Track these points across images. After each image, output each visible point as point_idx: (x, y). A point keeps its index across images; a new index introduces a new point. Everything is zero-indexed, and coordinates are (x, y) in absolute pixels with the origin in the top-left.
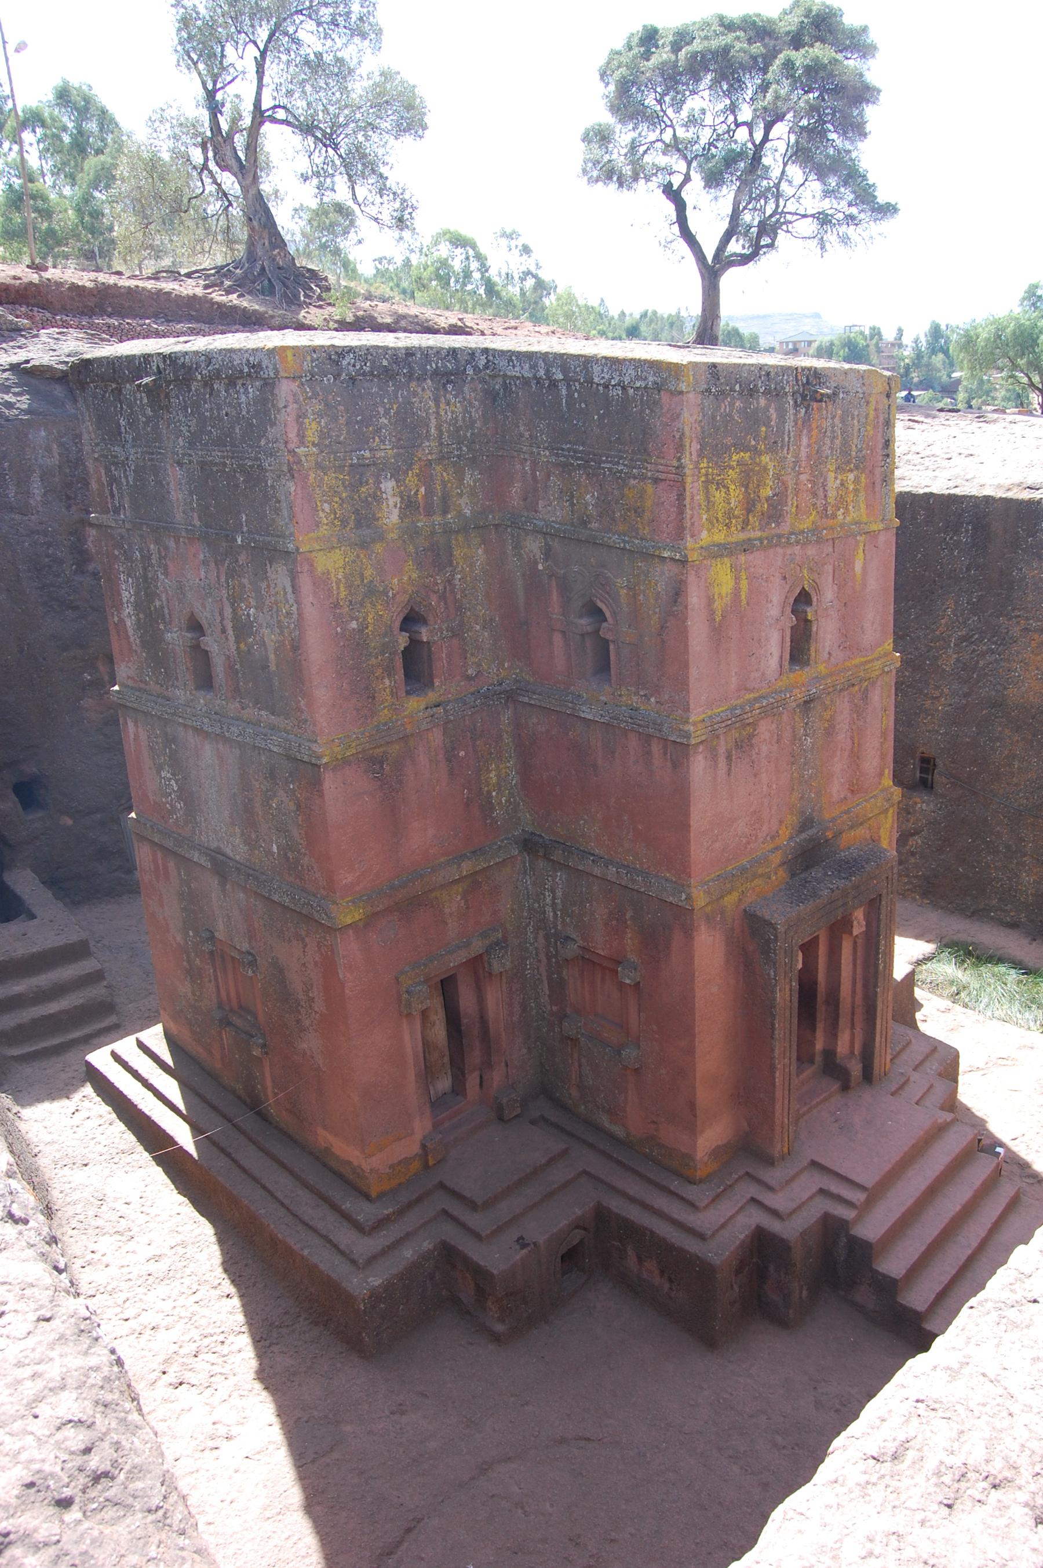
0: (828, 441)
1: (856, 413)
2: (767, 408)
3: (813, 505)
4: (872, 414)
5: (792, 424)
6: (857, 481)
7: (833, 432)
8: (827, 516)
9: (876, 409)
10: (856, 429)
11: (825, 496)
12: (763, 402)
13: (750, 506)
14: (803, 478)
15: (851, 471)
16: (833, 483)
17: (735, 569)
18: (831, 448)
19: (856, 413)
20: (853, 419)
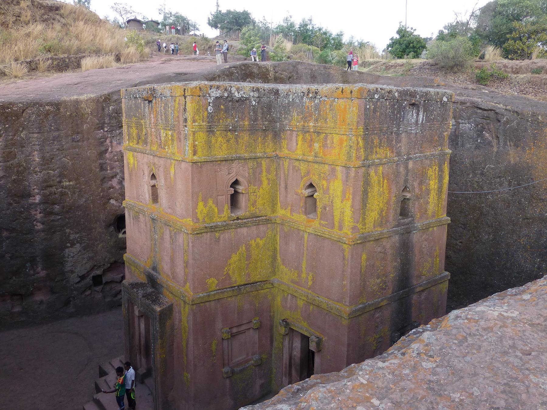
0: (159, 116)
1: (170, 106)
2: (141, 103)
3: (157, 141)
4: (177, 105)
5: (148, 109)
6: (172, 136)
7: (161, 113)
8: (162, 147)
9: (179, 104)
10: (170, 112)
11: (160, 139)
12: (140, 101)
13: (139, 138)
14: (153, 130)
15: (169, 130)
16: (163, 135)
17: (133, 156)
18: (162, 120)
19: (170, 106)
20: (168, 108)
